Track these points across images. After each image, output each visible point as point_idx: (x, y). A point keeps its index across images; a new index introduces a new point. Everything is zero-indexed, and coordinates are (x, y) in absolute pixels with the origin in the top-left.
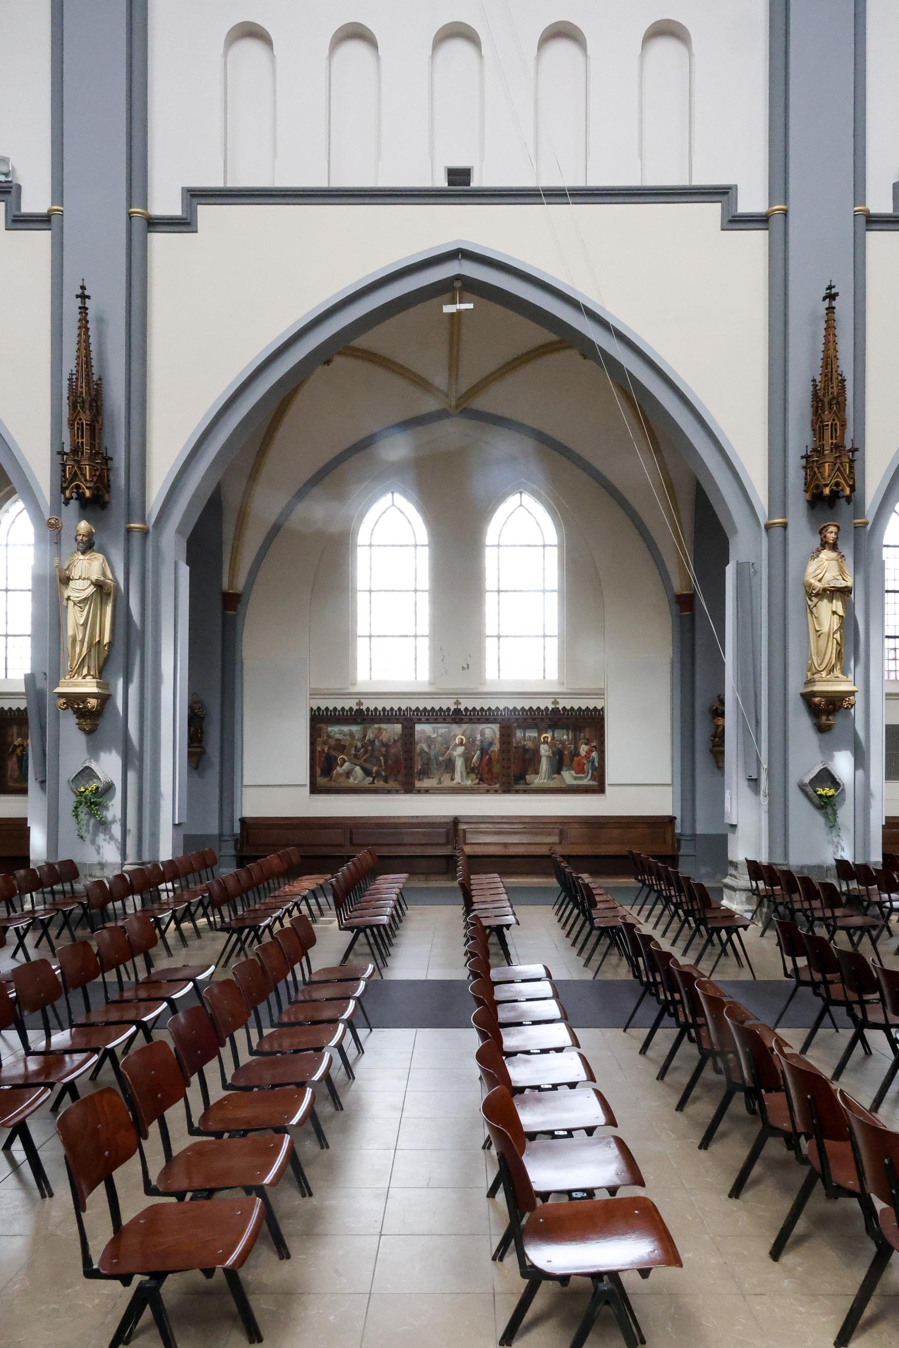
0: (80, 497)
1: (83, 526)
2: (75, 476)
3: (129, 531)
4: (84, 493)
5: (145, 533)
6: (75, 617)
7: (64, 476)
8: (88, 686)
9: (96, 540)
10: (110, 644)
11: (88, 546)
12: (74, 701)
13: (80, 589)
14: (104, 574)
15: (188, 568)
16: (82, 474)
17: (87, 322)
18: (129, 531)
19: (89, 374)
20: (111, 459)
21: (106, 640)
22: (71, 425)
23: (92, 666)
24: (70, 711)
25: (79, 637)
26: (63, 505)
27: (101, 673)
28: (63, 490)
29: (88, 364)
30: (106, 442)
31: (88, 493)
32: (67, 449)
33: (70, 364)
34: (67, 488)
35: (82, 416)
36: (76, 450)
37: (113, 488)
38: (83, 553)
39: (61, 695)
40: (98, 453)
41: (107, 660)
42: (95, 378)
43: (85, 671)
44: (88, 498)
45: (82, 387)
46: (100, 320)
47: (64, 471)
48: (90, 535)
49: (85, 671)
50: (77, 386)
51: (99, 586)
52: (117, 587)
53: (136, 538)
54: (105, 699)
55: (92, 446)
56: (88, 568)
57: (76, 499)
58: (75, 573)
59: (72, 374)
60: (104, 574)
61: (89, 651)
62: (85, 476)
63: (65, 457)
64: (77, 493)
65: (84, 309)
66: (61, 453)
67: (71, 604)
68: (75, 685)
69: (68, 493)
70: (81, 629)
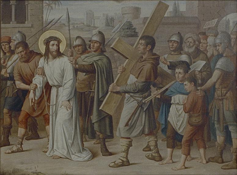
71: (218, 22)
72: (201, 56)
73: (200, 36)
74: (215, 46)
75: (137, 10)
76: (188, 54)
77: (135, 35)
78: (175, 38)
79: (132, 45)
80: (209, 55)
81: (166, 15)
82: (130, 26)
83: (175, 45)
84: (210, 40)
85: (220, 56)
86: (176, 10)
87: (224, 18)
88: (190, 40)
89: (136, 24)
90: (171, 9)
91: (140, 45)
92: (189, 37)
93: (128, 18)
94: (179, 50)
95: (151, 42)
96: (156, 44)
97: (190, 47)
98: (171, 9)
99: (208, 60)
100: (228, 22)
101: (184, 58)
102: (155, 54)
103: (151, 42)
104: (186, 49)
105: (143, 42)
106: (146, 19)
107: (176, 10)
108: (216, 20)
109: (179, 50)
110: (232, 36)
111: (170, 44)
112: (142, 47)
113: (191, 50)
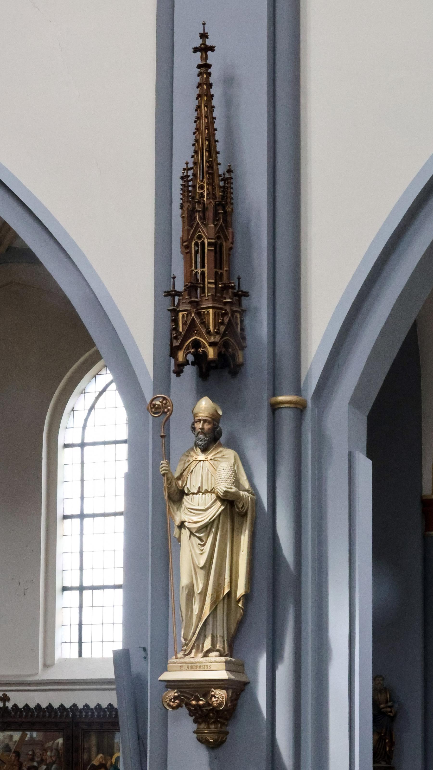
0: (200, 360)
1: (205, 406)
2: (191, 328)
3: (274, 408)
4: (205, 354)
5: (300, 409)
6: (191, 555)
7: (176, 329)
8: (214, 669)
9: (225, 428)
10: (247, 597)
11: (212, 438)
12: (191, 693)
13: (198, 509)
14: (237, 482)
15: (369, 463)
16: (203, 323)
17: (210, 86)
18: (274, 408)
19: (212, 165)
20: (246, 294)
21: (241, 590)
22: (186, 247)
23: (219, 633)
24: (184, 710)
25: (199, 588)
26: (173, 376)
27: (233, 647)
28: (173, 352)
29: (212, 150)
30: (239, 269)
31: (211, 353)
32: (180, 286)
33: (183, 153)
34: (179, 348)
35: (203, 231)
36: (193, 286)
37: (250, 341)
38: (204, 450)
39: (171, 684)
40: (226, 288)
41: (241, 623)
42: (221, 170)
43: (207, 645)
44: (213, 361)
45: (202, 187)
46: (229, 81)
47: (175, 321)
48: (215, 420)
49: (207, 645)
50: (194, 186)
51: (229, 501)
52: (257, 502)
53: (287, 417)
54: (239, 689)
55: (218, 277)
56: (211, 473)
57: (193, 364)
58: (193, 483)
59: (187, 169)
60: (237, 482)
61: (214, 611)
62: (207, 327)
63: (177, 298)
64: (195, 355)
65: (205, 68)
66: (171, 294)
67: (185, 533)
68: (192, 668)
69: (181, 356)
70: (201, 574)
71: (53, 743)
72: (44, 763)
73: (44, 752)
74: (51, 757)
75: (11, 737)
76: (38, 762)
77: (10, 750)
78: (30, 753)
79: (9, 756)
80: (48, 762)
81: (26, 739)
82: (7, 746)
83: (31, 756)
84: (49, 753)
85: (54, 763)
86: (31, 736)
87: (56, 741)
88: (38, 754)
89: (11, 745)
90: (28, 736)
91: (12, 755)
92: (38, 752)
93: (6, 741)
94: (32, 760)
95: (18, 754)
96: (21, 756)
97: (38, 758)
98: (28, 736)
99: (48, 765)
100: (58, 743)
101: (35, 764)
102: (20, 762)
103: (18, 754)
104: (36, 759)
105: (14, 755)
106: (16, 741)
107: (31, 736)
108: (51, 743)
109: (32, 760)
110: (60, 751)
111: (28, 756)
112: (13, 758)
113: (39, 759)
